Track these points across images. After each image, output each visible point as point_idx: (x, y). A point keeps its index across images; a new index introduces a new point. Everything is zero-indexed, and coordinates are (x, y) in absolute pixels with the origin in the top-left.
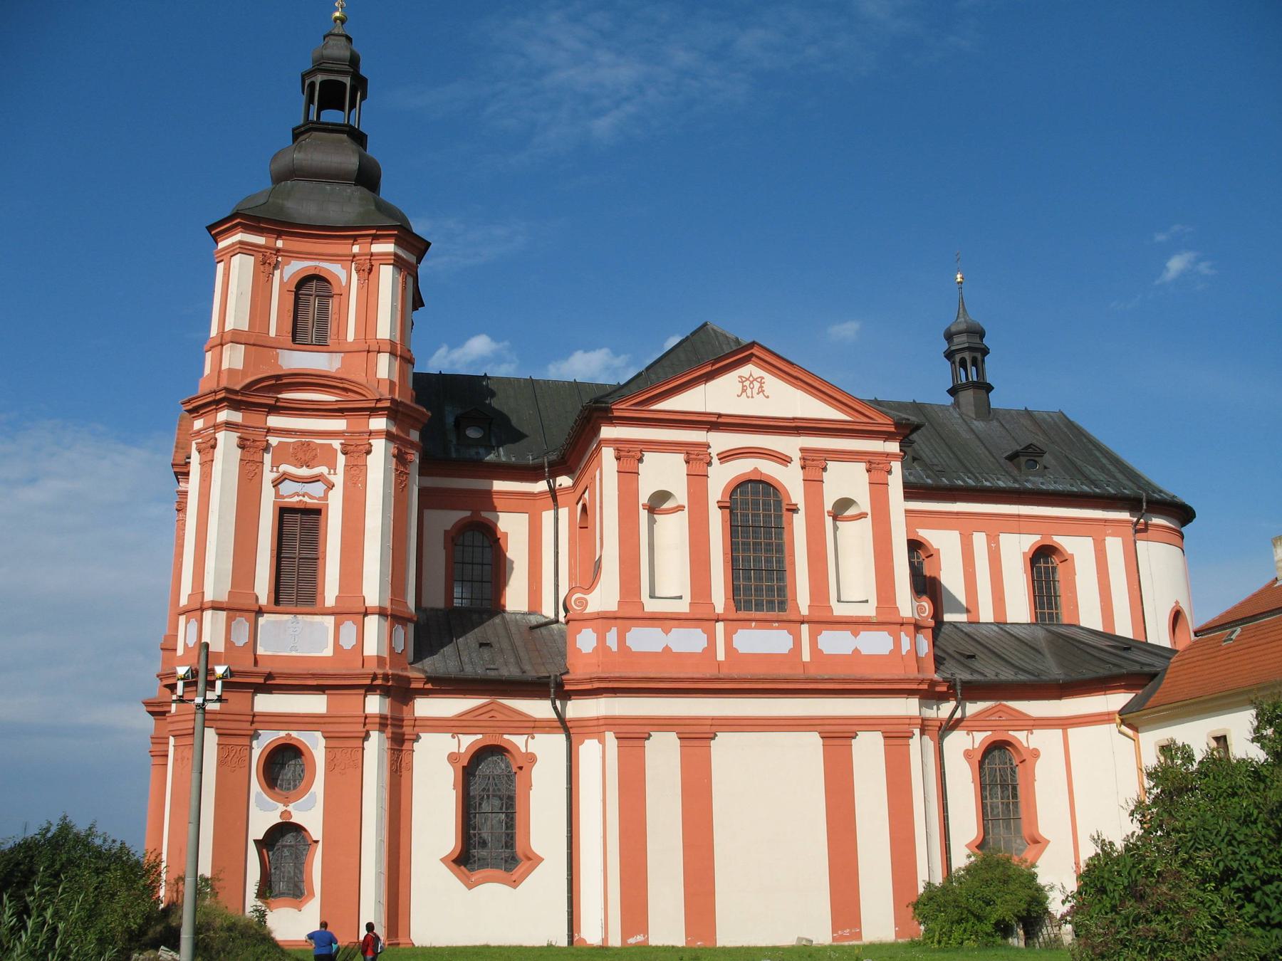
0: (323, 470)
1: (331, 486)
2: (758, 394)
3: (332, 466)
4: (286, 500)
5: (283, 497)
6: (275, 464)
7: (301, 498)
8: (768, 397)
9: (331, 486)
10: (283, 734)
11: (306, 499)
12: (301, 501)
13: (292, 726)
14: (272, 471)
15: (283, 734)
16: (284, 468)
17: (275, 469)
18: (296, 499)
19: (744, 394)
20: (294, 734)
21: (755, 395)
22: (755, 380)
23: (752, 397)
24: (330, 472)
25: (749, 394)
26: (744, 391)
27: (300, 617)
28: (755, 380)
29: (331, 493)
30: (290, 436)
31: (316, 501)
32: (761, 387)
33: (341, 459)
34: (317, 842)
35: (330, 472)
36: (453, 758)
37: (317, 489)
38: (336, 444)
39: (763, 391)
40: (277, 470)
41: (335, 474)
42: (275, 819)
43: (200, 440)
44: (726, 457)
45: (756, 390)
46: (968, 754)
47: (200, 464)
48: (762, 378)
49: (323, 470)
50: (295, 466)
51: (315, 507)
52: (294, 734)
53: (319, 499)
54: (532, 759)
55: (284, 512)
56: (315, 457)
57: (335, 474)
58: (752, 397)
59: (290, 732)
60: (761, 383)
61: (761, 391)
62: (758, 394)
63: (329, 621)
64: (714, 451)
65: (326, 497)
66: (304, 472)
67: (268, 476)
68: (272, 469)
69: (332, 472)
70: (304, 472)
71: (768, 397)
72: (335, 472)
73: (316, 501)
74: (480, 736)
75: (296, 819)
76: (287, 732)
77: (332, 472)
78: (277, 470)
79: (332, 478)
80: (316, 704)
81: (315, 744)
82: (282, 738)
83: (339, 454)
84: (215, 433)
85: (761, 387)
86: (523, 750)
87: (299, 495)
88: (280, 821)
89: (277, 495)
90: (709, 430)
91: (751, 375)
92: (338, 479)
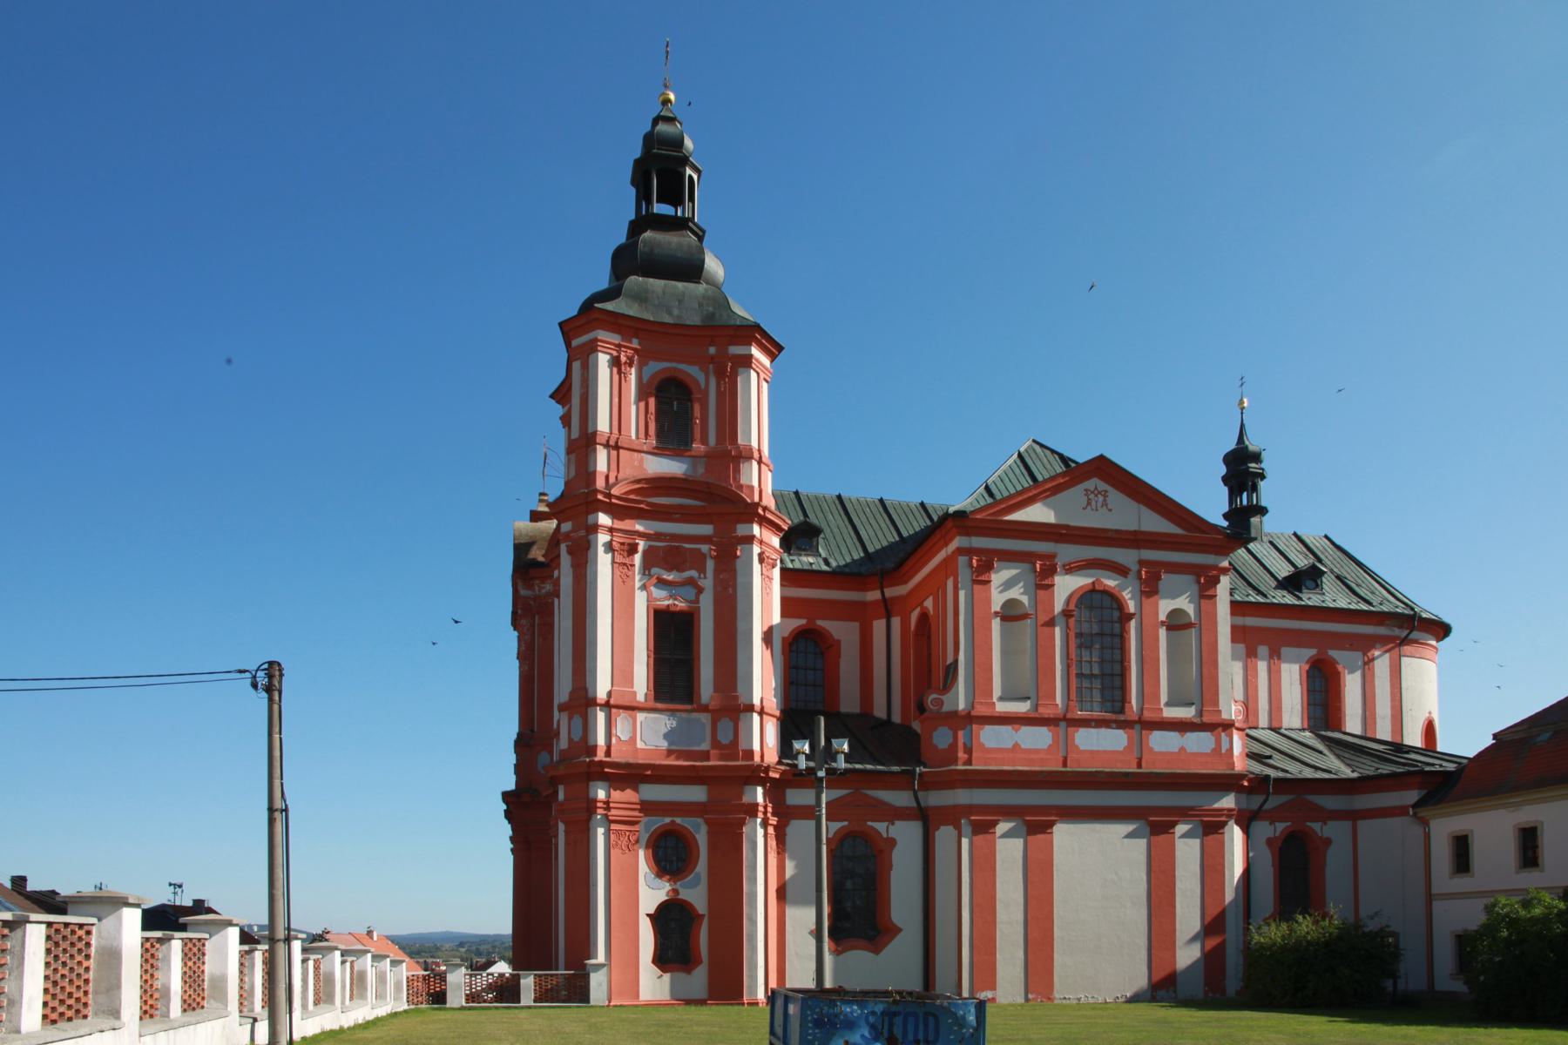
1: (700, 590)
2: (1102, 506)
3: (702, 570)
4: (658, 603)
8: (1110, 510)
9: (700, 590)
19: (1089, 507)
21: (1099, 508)
22: (1099, 493)
23: (1097, 510)
25: (1094, 507)
26: (1089, 503)
28: (1099, 493)
29: (702, 597)
32: (1105, 500)
33: (710, 565)
37: (690, 592)
38: (705, 548)
39: (1106, 505)
41: (705, 578)
44: (1070, 569)
45: (1099, 504)
46: (1270, 842)
48: (1106, 491)
49: (693, 573)
54: (892, 842)
57: (705, 578)
58: (1097, 510)
60: (1105, 496)
61: (1105, 504)
62: (1102, 506)
63: (705, 718)
64: (1059, 562)
65: (697, 601)
69: (702, 576)
71: (1110, 510)
72: (705, 575)
77: (702, 576)
84: (587, 535)
85: (1105, 500)
86: (885, 835)
89: (649, 599)
90: (1057, 541)
91: (1096, 488)
92: (708, 583)
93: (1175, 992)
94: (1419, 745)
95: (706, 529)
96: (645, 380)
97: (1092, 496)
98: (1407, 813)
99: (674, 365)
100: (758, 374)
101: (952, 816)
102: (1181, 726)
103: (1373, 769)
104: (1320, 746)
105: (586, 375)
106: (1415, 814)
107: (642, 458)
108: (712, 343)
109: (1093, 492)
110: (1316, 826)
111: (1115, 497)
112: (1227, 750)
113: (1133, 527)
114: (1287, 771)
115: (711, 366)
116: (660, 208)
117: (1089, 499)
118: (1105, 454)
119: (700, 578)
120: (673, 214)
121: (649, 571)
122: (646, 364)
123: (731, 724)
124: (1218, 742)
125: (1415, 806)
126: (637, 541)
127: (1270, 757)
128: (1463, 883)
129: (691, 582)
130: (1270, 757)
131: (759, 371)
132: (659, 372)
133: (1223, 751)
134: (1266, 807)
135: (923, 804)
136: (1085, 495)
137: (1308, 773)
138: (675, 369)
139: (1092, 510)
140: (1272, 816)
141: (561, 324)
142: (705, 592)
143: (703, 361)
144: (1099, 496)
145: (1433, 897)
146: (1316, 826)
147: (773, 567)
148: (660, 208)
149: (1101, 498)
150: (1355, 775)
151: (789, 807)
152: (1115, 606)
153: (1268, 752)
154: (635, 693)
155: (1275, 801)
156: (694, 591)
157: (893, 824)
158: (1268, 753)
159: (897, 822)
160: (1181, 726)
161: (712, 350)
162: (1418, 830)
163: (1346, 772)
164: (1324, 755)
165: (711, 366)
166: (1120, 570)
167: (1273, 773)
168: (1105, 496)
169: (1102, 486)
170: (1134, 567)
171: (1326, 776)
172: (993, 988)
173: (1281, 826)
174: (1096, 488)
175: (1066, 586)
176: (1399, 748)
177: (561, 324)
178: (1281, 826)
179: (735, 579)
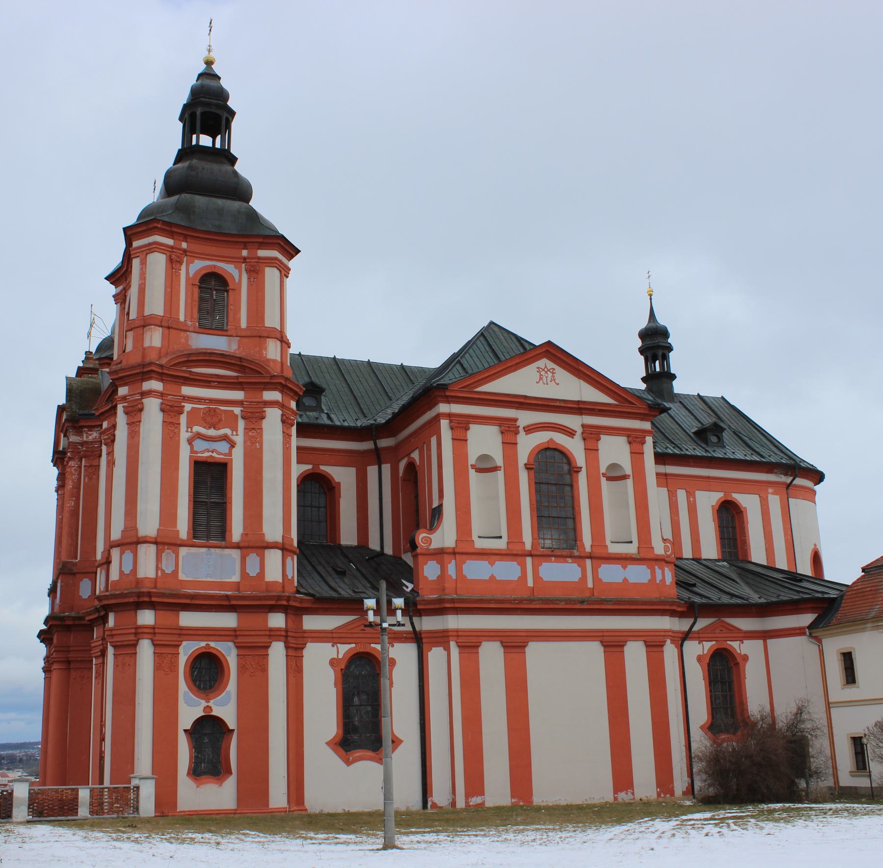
0: (227, 431)
1: (233, 445)
3: (235, 429)
5: (196, 452)
6: (189, 426)
7: (210, 454)
8: (558, 384)
9: (233, 445)
10: (203, 644)
11: (215, 455)
12: (211, 456)
13: (211, 638)
14: (187, 431)
15: (203, 644)
16: (196, 429)
17: (189, 430)
18: (206, 454)
19: (541, 381)
20: (212, 644)
21: (549, 382)
22: (549, 370)
23: (547, 384)
24: (233, 433)
26: (541, 379)
27: (213, 550)
28: (549, 370)
29: (234, 450)
30: (200, 403)
31: (222, 456)
33: (241, 424)
34: (233, 730)
35: (233, 433)
36: (333, 662)
37: (223, 447)
38: (237, 410)
39: (554, 380)
40: (191, 430)
42: (199, 713)
43: (126, 404)
44: (530, 429)
45: (549, 379)
47: (128, 424)
49: (227, 431)
50: (205, 428)
51: (222, 461)
52: (212, 644)
53: (225, 455)
56: (220, 420)
57: (237, 435)
58: (547, 384)
59: (209, 643)
60: (553, 373)
62: (551, 381)
63: (236, 554)
65: (230, 454)
66: (212, 432)
67: (184, 435)
68: (187, 429)
70: (212, 432)
71: (558, 384)
72: (237, 431)
73: (222, 456)
74: (353, 645)
75: (216, 712)
76: (206, 643)
78: (191, 430)
79: (234, 438)
80: (228, 620)
81: (229, 654)
82: (202, 647)
83: (240, 419)
84: (141, 399)
88: (203, 714)
89: (192, 451)
90: (517, 408)
91: (546, 367)
92: (239, 439)
93: (633, 794)
94: (810, 574)
95: (238, 395)
96: (191, 275)
97: (543, 373)
98: (804, 634)
100: (280, 271)
101: (442, 638)
102: (624, 560)
103: (775, 595)
104: (734, 576)
105: (144, 270)
106: (810, 634)
107: (188, 336)
108: (245, 248)
109: (543, 370)
110: (735, 645)
111: (561, 374)
112: (661, 581)
113: (576, 398)
114: (709, 598)
115: (243, 265)
116: (205, 141)
117: (541, 375)
118: (551, 340)
119: (233, 435)
120: (211, 145)
121: (192, 428)
122: (193, 262)
123: (258, 559)
124: (653, 573)
125: (812, 626)
126: (183, 404)
127: (694, 585)
128: (851, 693)
130: (694, 585)
131: (281, 269)
132: (201, 269)
133: (658, 582)
134: (695, 629)
135: (417, 629)
136: (538, 372)
137: (726, 599)
138: (215, 266)
139: (544, 383)
140: (701, 637)
141: (125, 229)
142: (236, 446)
143: (237, 261)
144: (548, 372)
145: (831, 706)
146: (735, 645)
147: (292, 426)
148: (205, 141)
149: (550, 374)
150: (763, 600)
151: (305, 632)
152: (565, 461)
153: (692, 580)
154: (178, 532)
155: (702, 623)
156: (229, 446)
157: (393, 646)
158: (693, 582)
159: (395, 644)
160: (624, 560)
161: (245, 253)
162: (813, 648)
163: (755, 598)
164: (737, 583)
165: (243, 265)
166: (570, 433)
167: (697, 599)
168: (553, 373)
169: (550, 365)
170: (579, 430)
171: (739, 601)
172: (482, 793)
173: (708, 645)
174: (546, 367)
175: (527, 444)
176: (794, 577)
177: (125, 229)
178: (708, 645)
179: (261, 436)
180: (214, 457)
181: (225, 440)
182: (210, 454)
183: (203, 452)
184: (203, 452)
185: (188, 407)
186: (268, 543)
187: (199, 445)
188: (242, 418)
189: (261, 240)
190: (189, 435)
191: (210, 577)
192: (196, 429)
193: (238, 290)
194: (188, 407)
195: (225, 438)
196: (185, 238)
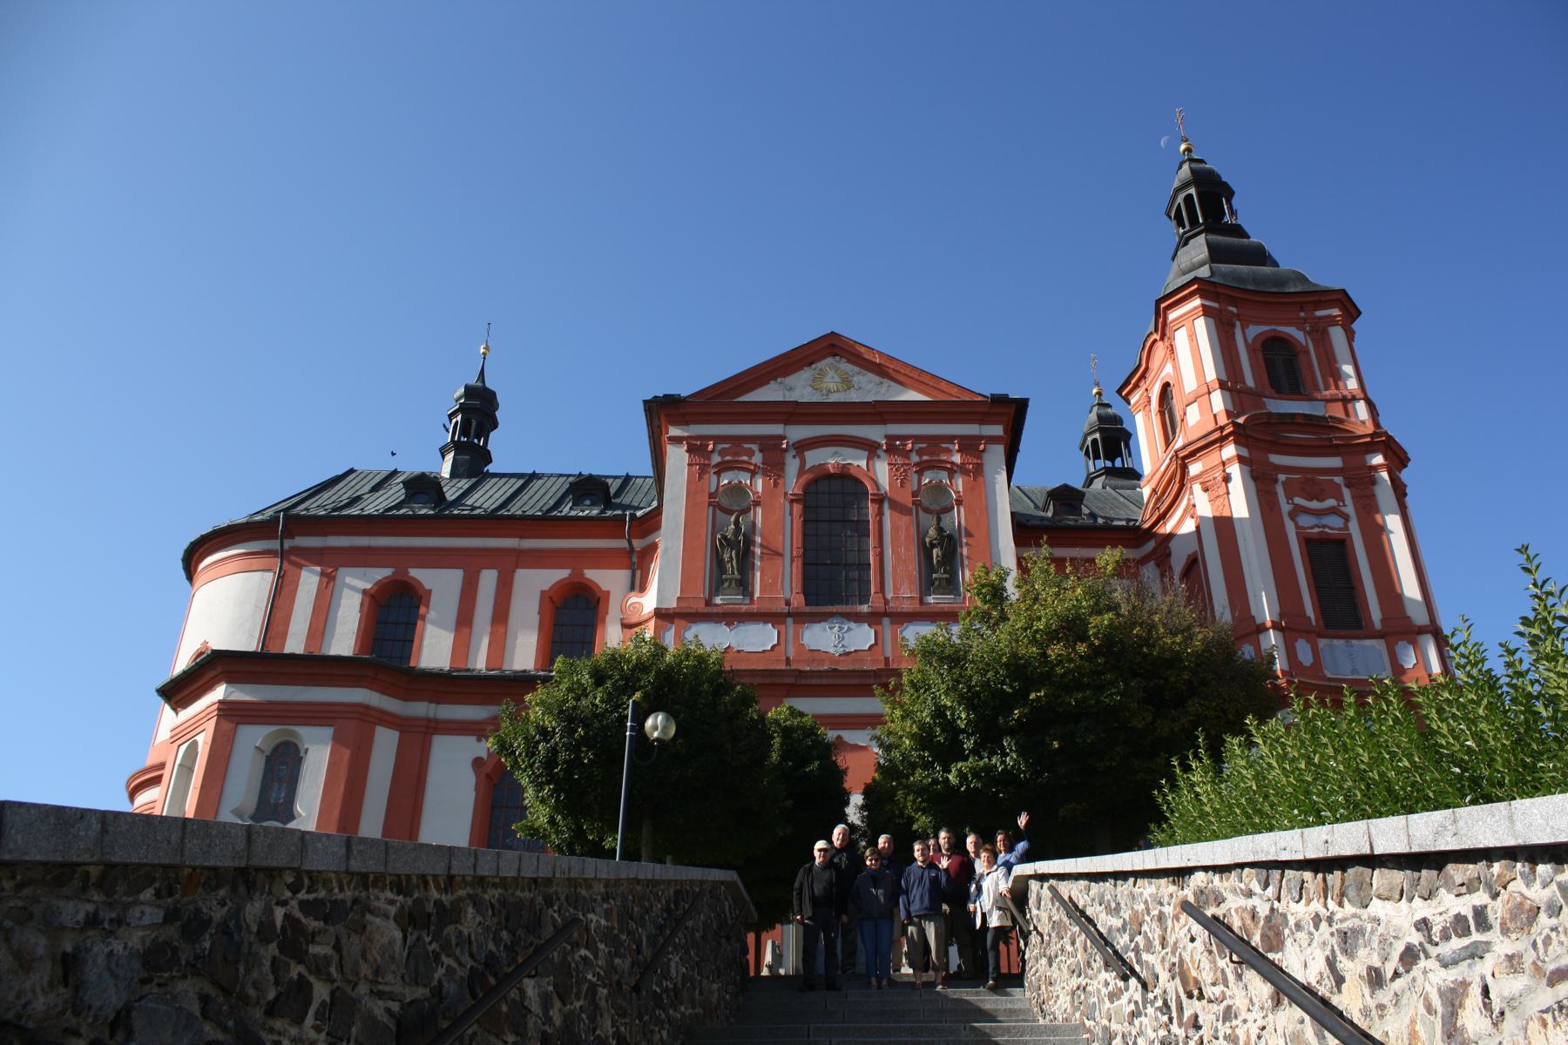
0: (1331, 502)
1: (1346, 518)
3: (1340, 498)
5: (1303, 528)
6: (1289, 497)
7: (1321, 529)
11: (1327, 530)
16: (1298, 500)
18: (1316, 530)
33: (1347, 493)
37: (1335, 522)
38: (1338, 480)
49: (1331, 502)
53: (1339, 529)
55: (1312, 545)
57: (1345, 506)
63: (1379, 645)
65: (1346, 528)
66: (1314, 505)
67: (1286, 508)
69: (1341, 504)
70: (1314, 505)
72: (1343, 501)
79: (1343, 509)
87: (1319, 527)
89: (1297, 526)
92: (1349, 509)
95: (1335, 462)
96: (1250, 341)
99: (1274, 327)
108: (1302, 309)
129: (1333, 511)
138: (1275, 330)
161: (1302, 314)
180: (1327, 533)
181: (1334, 513)
182: (1321, 529)
183: (1312, 528)
184: (1312, 528)
185: (1282, 477)
186: (1420, 627)
187: (1305, 520)
188: (1348, 486)
189: (1317, 298)
190: (1291, 507)
191: (1358, 674)
192: (1298, 500)
193: (1307, 352)
194: (1282, 477)
195: (1333, 511)
196: (1234, 303)
